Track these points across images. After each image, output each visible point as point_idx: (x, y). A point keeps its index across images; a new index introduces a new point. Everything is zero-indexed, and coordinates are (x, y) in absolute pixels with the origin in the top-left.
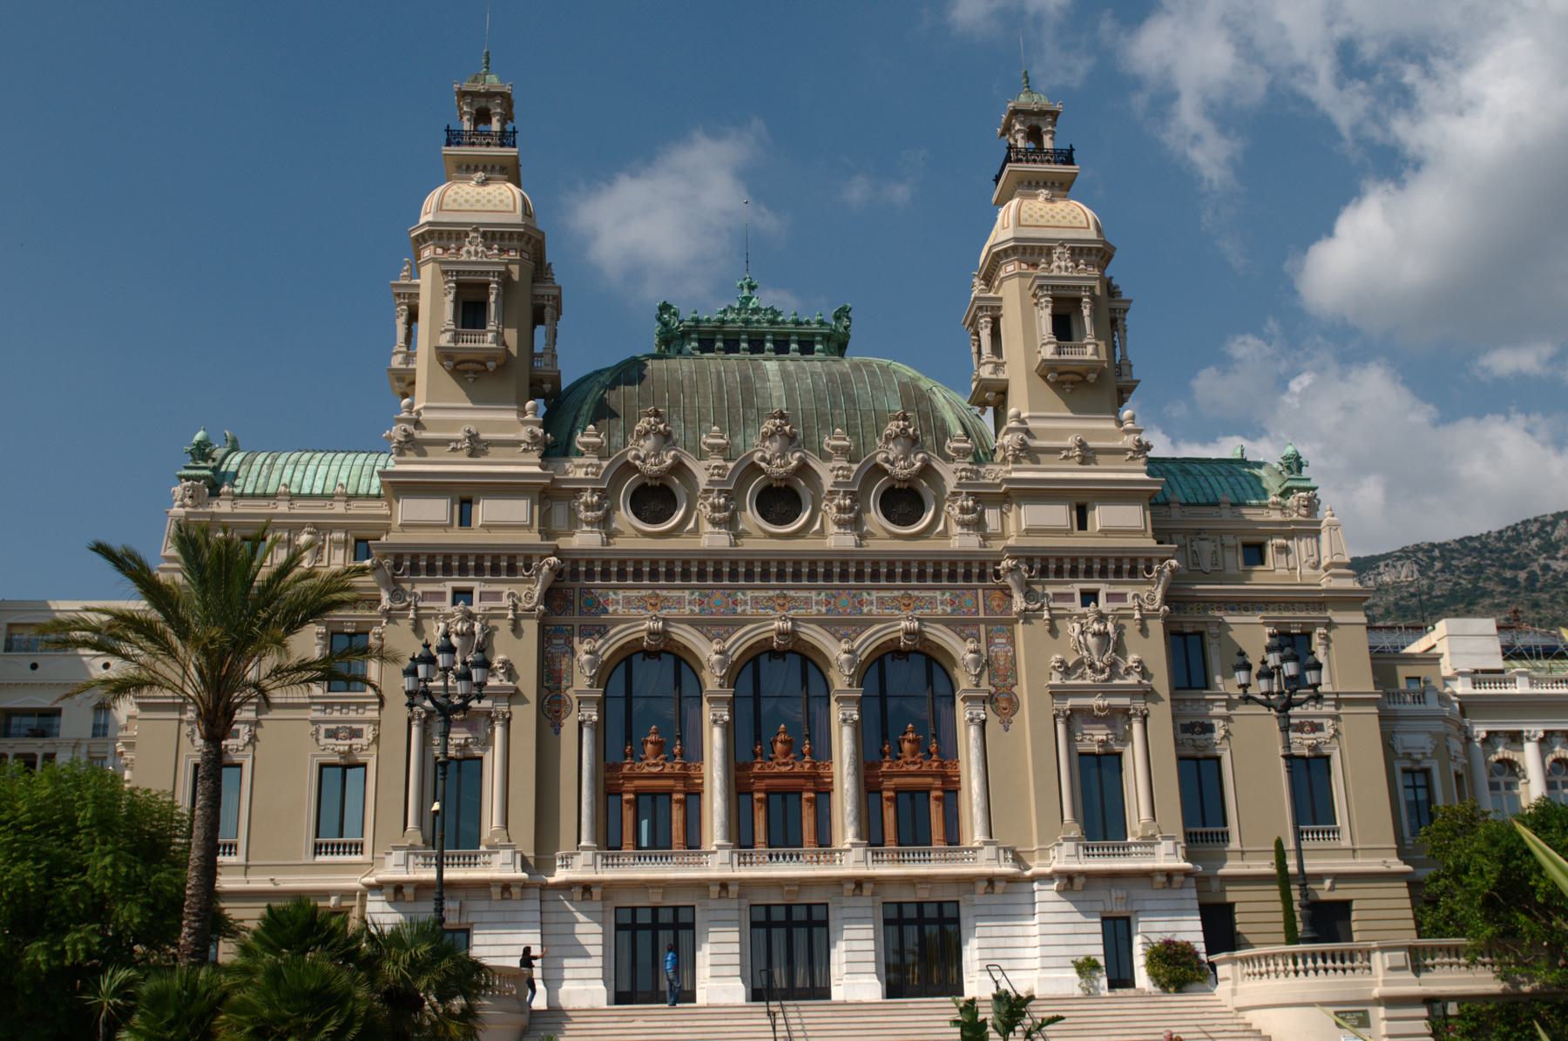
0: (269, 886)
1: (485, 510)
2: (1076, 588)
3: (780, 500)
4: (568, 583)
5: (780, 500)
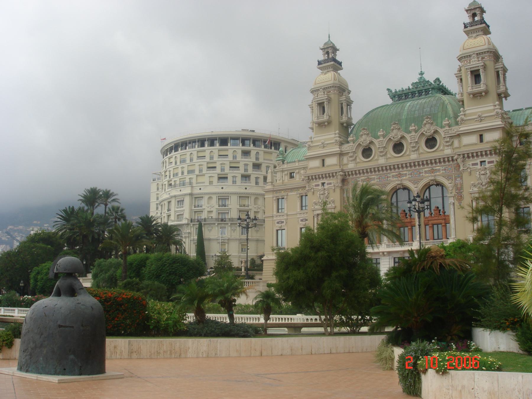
1: (329, 161)
2: (478, 161)
4: (348, 177)
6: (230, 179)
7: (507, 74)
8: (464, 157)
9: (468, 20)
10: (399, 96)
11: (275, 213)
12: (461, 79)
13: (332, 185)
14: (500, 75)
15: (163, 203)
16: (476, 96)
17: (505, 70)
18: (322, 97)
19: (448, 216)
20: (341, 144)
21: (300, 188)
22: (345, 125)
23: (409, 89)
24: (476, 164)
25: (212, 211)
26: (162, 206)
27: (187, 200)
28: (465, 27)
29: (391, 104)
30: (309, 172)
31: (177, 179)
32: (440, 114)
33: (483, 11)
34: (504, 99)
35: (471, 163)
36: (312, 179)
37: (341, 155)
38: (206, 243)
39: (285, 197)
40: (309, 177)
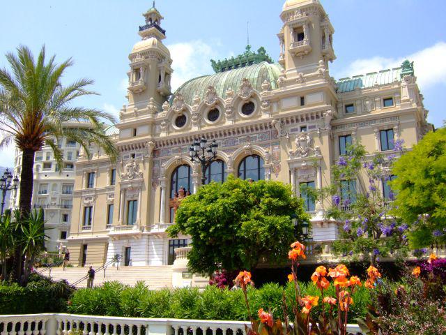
3: (213, 114)
5: (213, 114)
8: (282, 122)
12: (284, 41)
20: (156, 113)
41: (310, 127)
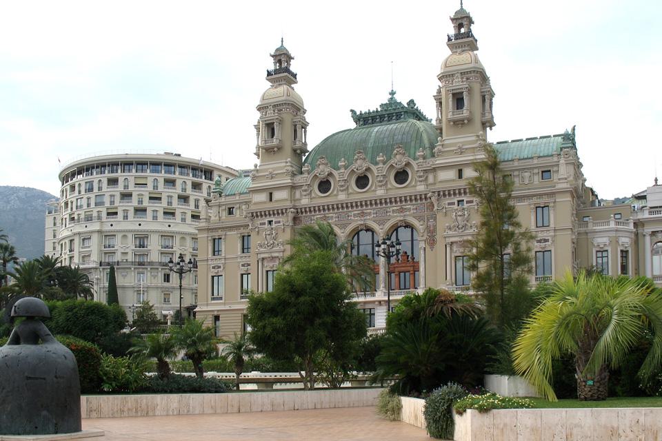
0: (229, 308)
1: (278, 195)
6: (149, 213)
7: (494, 100)
8: (439, 195)
9: (452, 32)
10: (364, 120)
11: (210, 256)
12: (441, 103)
13: (282, 224)
14: (487, 97)
15: (63, 242)
16: (458, 124)
17: (492, 95)
18: (271, 115)
19: (418, 263)
20: (294, 175)
21: (242, 226)
22: (298, 151)
23: (377, 111)
24: (453, 204)
25: (127, 253)
26: (62, 245)
27: (95, 239)
28: (449, 39)
29: (355, 129)
30: (253, 208)
31: (82, 213)
32: (413, 143)
33: (471, 22)
34: (488, 129)
35: (447, 202)
36: (257, 216)
37: (293, 188)
38: (119, 292)
39: (223, 237)
40: (252, 213)
41: (468, 202)
